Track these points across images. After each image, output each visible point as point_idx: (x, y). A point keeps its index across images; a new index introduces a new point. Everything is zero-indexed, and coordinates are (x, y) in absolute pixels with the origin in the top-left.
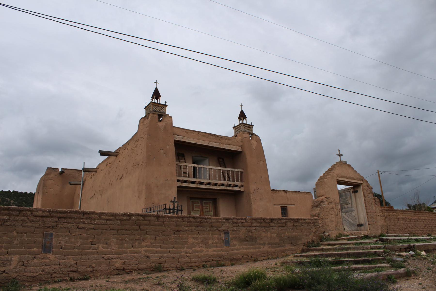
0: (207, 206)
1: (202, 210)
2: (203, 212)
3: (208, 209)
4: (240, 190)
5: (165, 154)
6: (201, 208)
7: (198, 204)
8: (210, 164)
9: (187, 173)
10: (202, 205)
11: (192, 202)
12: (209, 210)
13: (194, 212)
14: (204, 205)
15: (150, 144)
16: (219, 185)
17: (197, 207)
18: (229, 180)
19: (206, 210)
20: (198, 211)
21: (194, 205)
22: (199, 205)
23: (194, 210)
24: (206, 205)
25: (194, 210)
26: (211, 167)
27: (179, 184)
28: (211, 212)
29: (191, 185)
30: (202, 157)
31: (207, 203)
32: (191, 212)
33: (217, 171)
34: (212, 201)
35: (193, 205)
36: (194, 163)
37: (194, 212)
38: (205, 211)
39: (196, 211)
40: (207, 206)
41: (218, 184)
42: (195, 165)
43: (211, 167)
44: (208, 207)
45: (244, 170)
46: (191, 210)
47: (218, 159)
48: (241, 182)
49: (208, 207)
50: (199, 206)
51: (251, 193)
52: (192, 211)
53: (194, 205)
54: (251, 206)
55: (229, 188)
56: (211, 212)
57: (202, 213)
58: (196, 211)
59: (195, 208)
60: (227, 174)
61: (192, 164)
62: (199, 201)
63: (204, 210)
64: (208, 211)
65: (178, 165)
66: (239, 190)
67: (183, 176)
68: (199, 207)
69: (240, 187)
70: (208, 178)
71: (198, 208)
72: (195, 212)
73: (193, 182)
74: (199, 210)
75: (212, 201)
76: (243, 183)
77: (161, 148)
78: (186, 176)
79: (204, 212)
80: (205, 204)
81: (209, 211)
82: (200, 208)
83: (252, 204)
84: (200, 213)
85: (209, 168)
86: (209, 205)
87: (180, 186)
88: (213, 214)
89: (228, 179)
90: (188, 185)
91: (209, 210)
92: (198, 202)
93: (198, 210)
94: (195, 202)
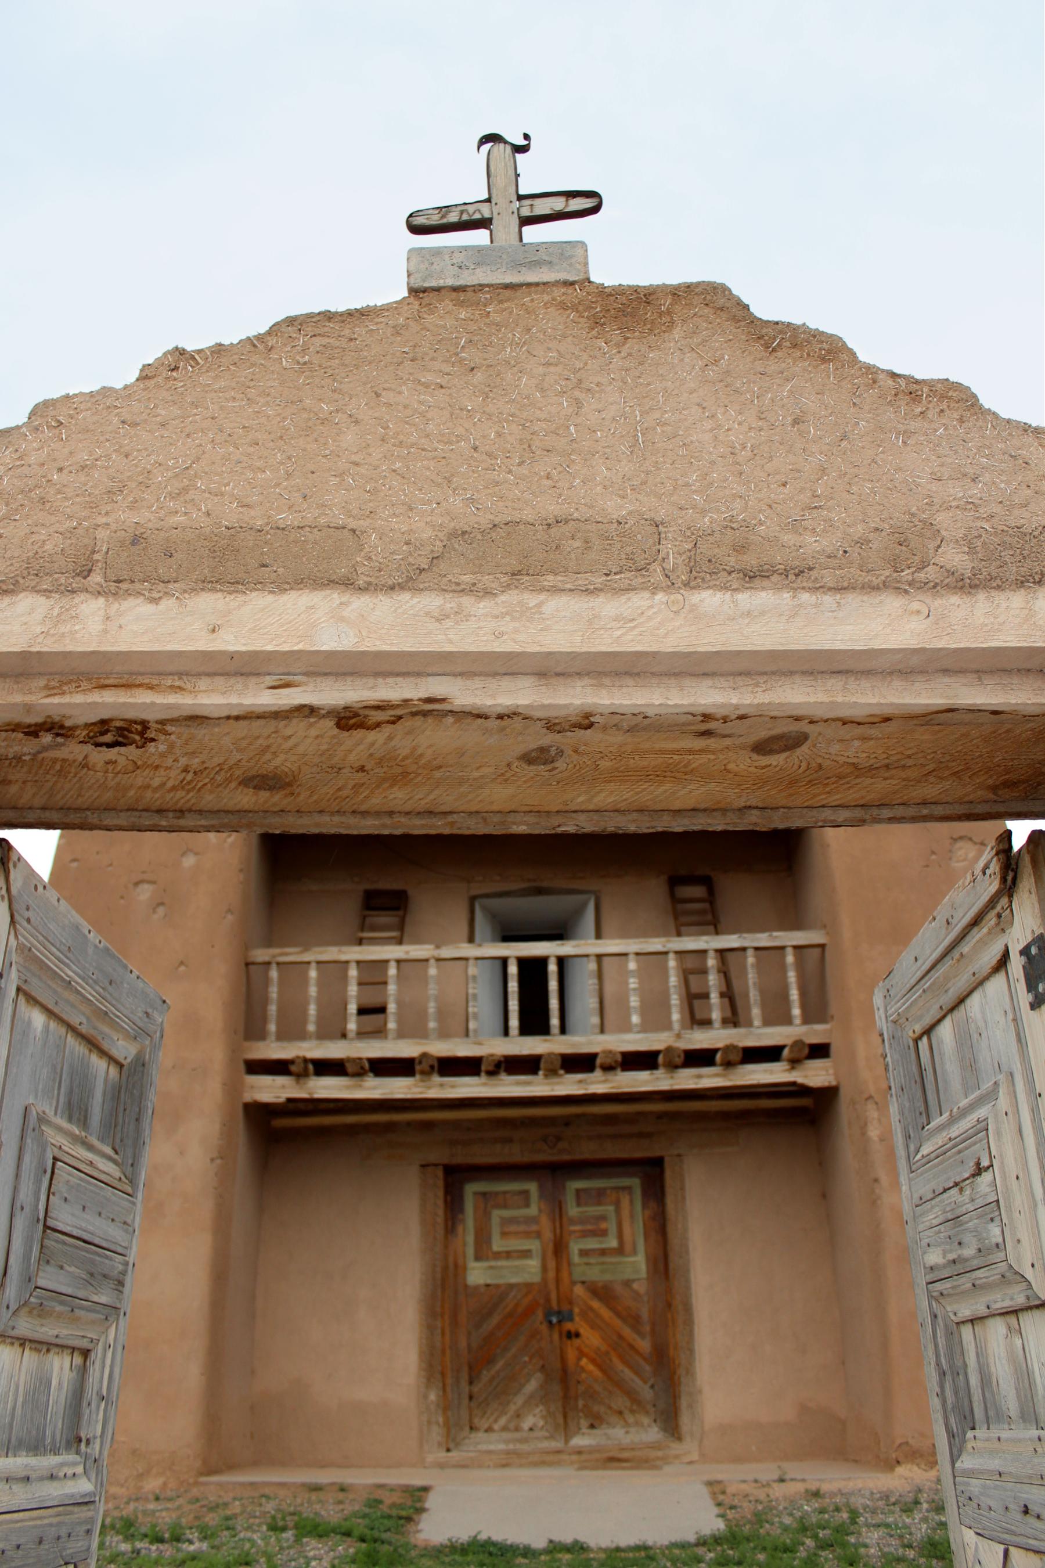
0: (603, 1218)
1: (559, 1248)
2: (569, 1264)
3: (604, 1233)
4: (800, 1080)
5: (162, 904)
6: (548, 1235)
7: (527, 1205)
8: (606, 927)
9: (392, 1007)
10: (557, 1210)
11: (475, 1194)
12: (613, 1243)
13: (491, 1267)
14: (573, 1210)
15: (75, 864)
16: (608, 1068)
17: (512, 1228)
18: (734, 1018)
19: (592, 1244)
20: (526, 1254)
21: (497, 1215)
22: (533, 1210)
23: (495, 1248)
24: (593, 1210)
25: (495, 1248)
26: (611, 946)
27: (283, 1087)
28: (634, 1252)
29: (374, 1088)
30: (539, 891)
31: (599, 1196)
32: (472, 1264)
33: (632, 965)
34: (635, 1183)
35: (490, 1219)
36: (508, 937)
37: (491, 1267)
38: (584, 1253)
39: (508, 1255)
40: (603, 1218)
41: (598, 1061)
42: (407, 953)
43: (611, 946)
44: (603, 1225)
45: (828, 933)
46: (470, 1251)
47: (674, 882)
48: (807, 1020)
49: (603, 1225)
50: (534, 1220)
51: (870, 1097)
52: (478, 1258)
53: (497, 1215)
54: (874, 1203)
55: (699, 1077)
56: (632, 1259)
57: (558, 1270)
58: (508, 1255)
59: (504, 1234)
60: (725, 972)
61: (494, 940)
62: (533, 1187)
63: (575, 1247)
64: (603, 1252)
65: (278, 964)
66: (794, 1084)
67: (361, 1034)
68: (534, 1228)
69: (795, 1063)
70: (595, 1020)
71: (527, 1235)
72: (500, 1263)
73: (526, 1065)
74: (534, 1245)
75: (635, 1183)
76: (816, 1033)
77: (145, 877)
78: (380, 1032)
79: (576, 1258)
80: (579, 1205)
81: (620, 1251)
82: (538, 1235)
83: (876, 1180)
84: (544, 1269)
85: (599, 957)
86: (617, 1204)
87: (290, 1100)
88: (643, 1267)
89: (729, 1014)
90: (348, 1087)
91: (613, 1243)
92: (526, 1193)
93: (530, 1251)
94: (505, 1193)
